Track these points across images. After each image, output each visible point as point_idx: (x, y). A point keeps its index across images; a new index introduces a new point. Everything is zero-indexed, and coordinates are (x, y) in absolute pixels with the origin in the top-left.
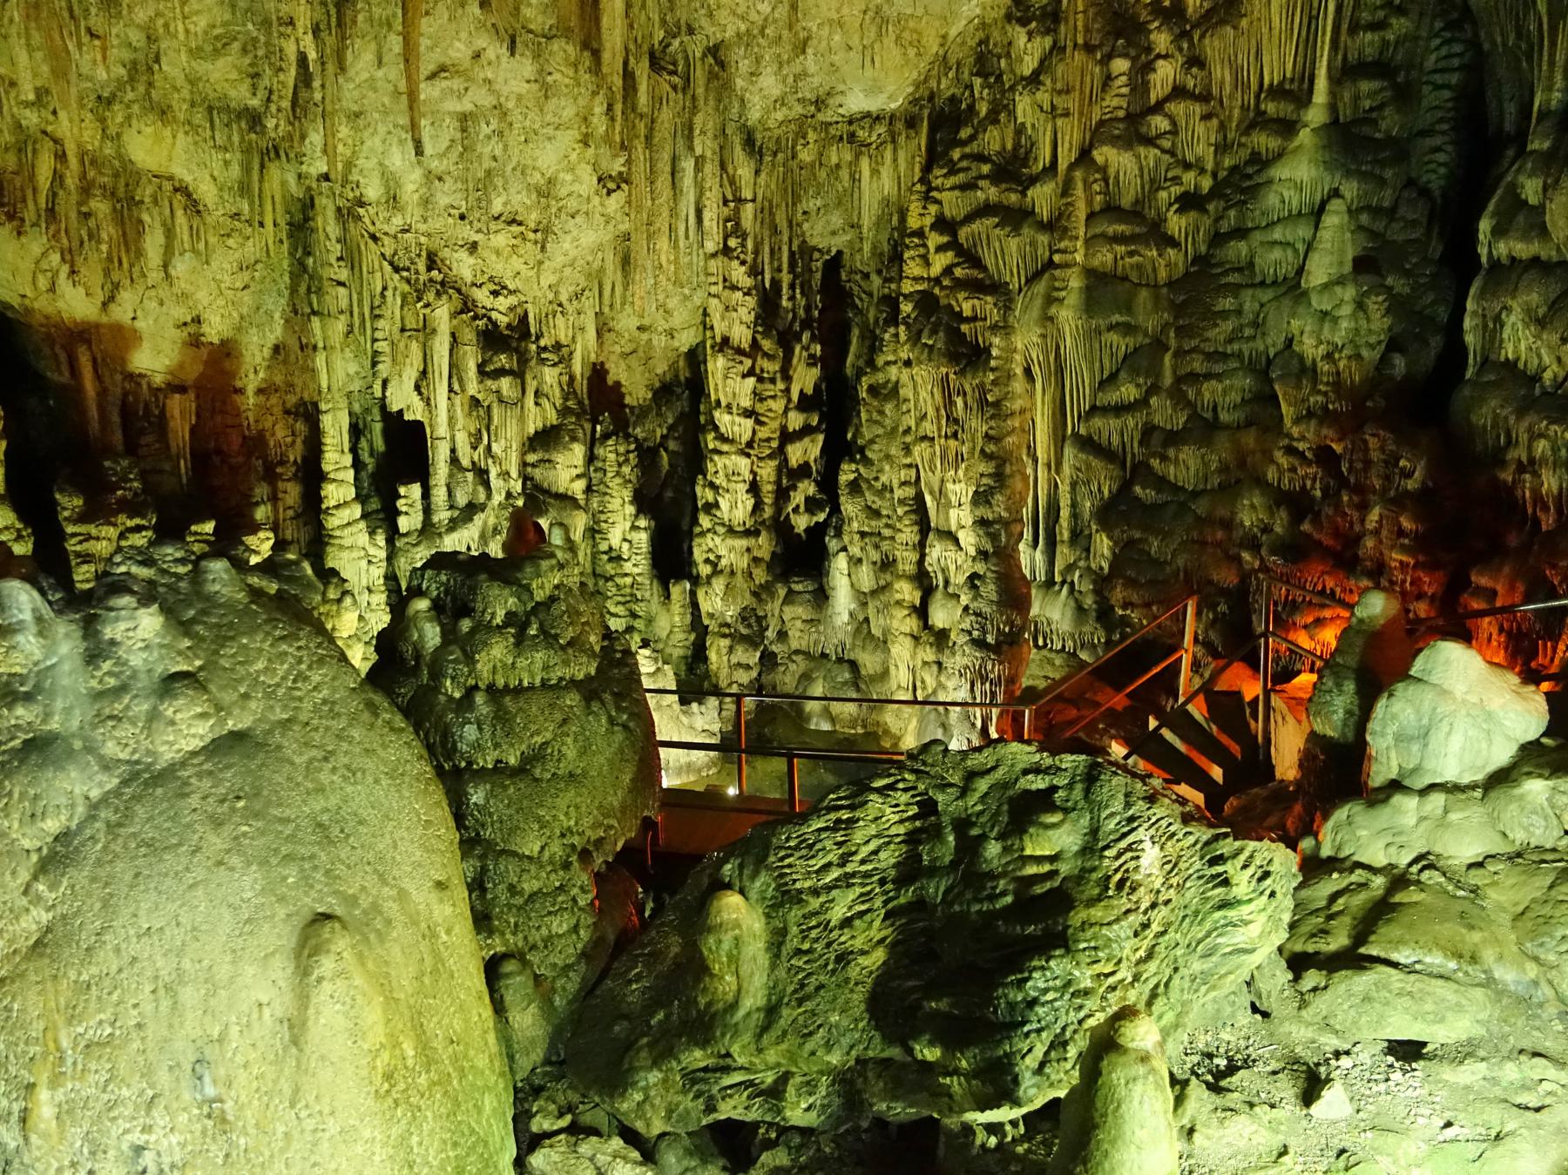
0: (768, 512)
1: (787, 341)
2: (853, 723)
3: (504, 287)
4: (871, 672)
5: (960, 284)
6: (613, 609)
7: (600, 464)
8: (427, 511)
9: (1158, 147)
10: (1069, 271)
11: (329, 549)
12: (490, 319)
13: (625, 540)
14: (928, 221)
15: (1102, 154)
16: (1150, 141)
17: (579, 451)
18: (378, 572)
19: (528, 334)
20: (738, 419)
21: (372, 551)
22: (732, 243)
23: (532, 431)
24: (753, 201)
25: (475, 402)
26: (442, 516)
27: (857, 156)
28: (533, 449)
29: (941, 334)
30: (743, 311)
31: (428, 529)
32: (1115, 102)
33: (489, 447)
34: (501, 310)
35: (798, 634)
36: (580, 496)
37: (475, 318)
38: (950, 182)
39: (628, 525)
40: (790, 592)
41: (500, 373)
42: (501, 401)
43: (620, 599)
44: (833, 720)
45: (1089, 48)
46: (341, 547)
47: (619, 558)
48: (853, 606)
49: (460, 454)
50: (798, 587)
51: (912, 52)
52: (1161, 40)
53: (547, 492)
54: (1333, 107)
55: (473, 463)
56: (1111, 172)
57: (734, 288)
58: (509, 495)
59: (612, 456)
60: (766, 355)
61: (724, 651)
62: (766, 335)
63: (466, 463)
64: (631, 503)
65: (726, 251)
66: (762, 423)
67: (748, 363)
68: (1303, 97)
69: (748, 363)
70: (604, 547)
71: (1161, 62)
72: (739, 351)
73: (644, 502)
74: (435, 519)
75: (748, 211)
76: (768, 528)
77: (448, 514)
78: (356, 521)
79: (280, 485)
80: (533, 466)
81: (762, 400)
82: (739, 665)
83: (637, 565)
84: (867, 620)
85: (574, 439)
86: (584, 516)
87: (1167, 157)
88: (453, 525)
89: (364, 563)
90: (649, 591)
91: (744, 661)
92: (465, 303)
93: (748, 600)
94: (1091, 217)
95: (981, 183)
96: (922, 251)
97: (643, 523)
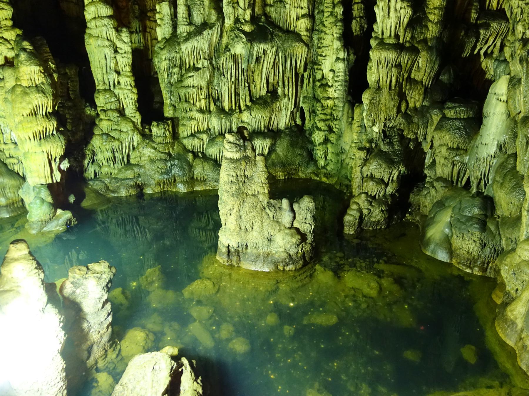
0: (432, 31)
2: (471, 262)
4: (506, 214)
6: (321, 125)
7: (321, 8)
8: (175, 27)
11: (86, 37)
13: (332, 70)
18: (125, 61)
21: (119, 44)
26: (183, 29)
31: (173, 40)
35: (442, 161)
36: (303, 33)
39: (334, 57)
40: (444, 117)
43: (322, 116)
44: (451, 252)
46: (91, 35)
47: (327, 85)
48: (502, 139)
50: (450, 114)
53: (281, 29)
58: (237, 21)
61: (359, 163)
64: (339, 39)
70: (319, 76)
73: (348, 40)
74: (178, 32)
76: (429, 49)
77: (188, 28)
78: (101, 18)
79: (148, 23)
80: (271, 6)
82: (372, 178)
83: (336, 91)
84: (515, 155)
86: (305, 49)
88: (190, 36)
89: (109, 52)
90: (341, 112)
91: (378, 175)
93: (399, 121)
97: (342, 55)
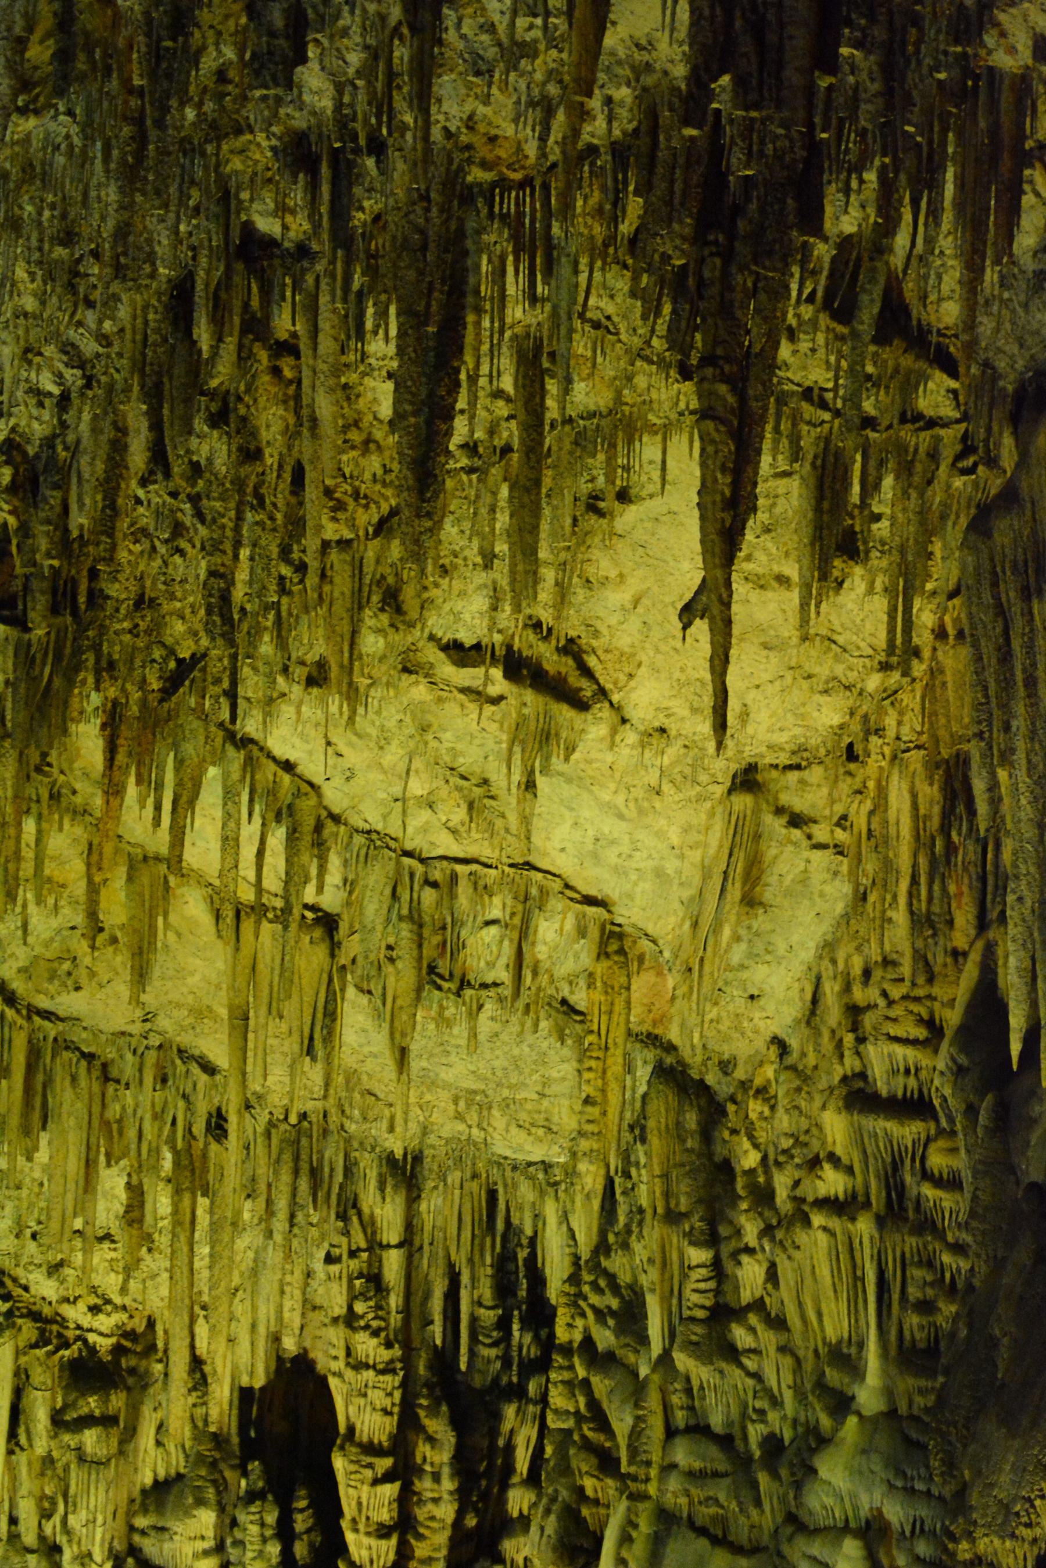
1: (474, 1410)
3: (108, 1302)
5: (587, 1445)
9: (741, 1365)
10: (641, 1506)
12: (85, 1341)
14: (578, 1337)
15: (682, 1360)
16: (732, 1353)
17: (206, 1519)
19: (152, 1348)
20: (366, 1541)
22: (360, 1307)
23: (149, 1481)
24: (400, 1245)
25: (48, 1461)
27: (542, 1193)
28: (145, 1510)
29: (553, 1518)
30: (378, 1397)
32: (695, 1298)
33: (64, 1521)
34: (102, 1331)
37: (67, 1345)
38: (594, 1299)
41: (87, 1421)
42: (82, 1459)
45: (672, 1217)
49: (22, 1527)
51: (541, 1132)
52: (751, 1230)
54: (889, 1393)
55: (42, 1538)
56: (695, 1384)
57: (359, 1366)
59: (254, 1529)
60: (431, 1440)
62: (433, 1411)
63: (29, 1538)
65: (350, 1320)
66: (420, 1537)
67: (385, 1463)
68: (855, 1369)
69: (385, 1463)
71: (745, 1259)
72: (372, 1449)
75: (393, 1264)
80: (143, 1533)
81: (421, 1502)
85: (200, 1502)
87: (750, 1382)
92: (42, 1331)
94: (671, 1433)
95: (611, 1322)
96: (566, 1375)
